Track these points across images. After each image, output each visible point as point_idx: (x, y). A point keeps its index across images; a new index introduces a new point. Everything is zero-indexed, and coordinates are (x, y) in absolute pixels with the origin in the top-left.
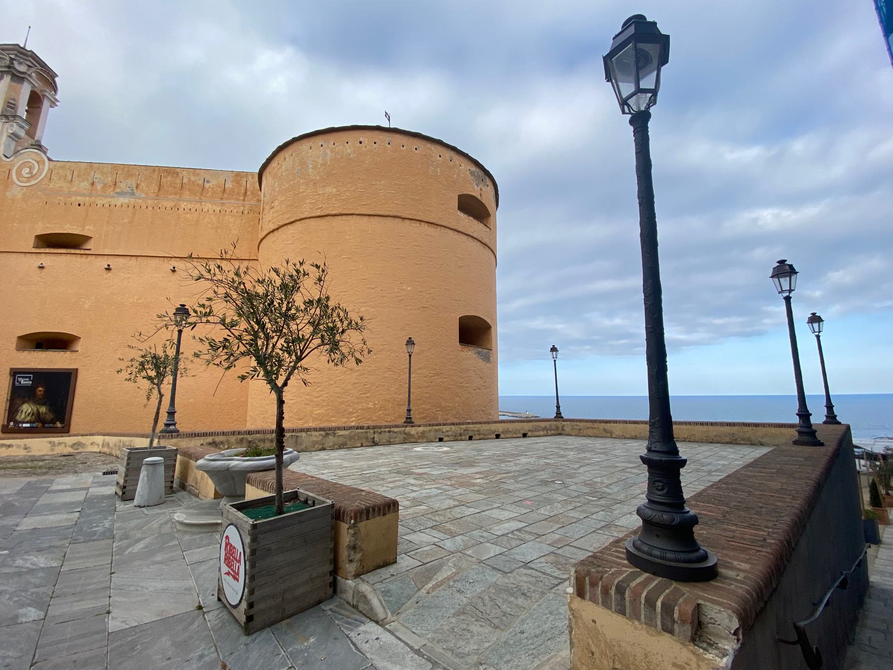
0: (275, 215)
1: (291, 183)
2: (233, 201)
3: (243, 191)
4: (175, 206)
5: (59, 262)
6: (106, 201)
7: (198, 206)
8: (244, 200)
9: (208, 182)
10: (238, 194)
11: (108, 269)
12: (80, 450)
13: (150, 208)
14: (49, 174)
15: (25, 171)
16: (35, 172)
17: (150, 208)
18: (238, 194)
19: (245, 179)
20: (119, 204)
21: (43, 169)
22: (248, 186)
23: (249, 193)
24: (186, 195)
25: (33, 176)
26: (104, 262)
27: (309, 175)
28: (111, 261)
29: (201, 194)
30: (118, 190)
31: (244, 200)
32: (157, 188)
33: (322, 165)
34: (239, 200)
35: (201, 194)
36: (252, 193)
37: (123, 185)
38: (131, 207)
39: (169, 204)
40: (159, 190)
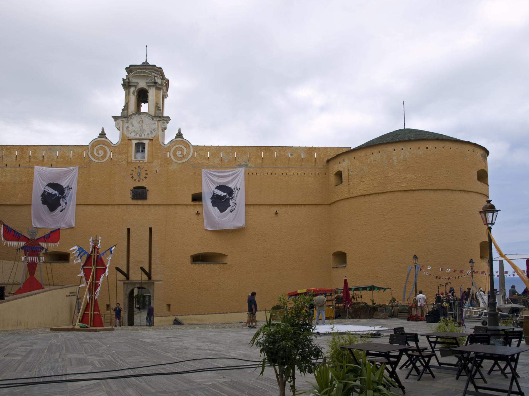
3: (314, 160)
15: (179, 153)
16: (185, 154)
23: (317, 161)
25: (184, 157)
29: (289, 164)
35: (289, 164)
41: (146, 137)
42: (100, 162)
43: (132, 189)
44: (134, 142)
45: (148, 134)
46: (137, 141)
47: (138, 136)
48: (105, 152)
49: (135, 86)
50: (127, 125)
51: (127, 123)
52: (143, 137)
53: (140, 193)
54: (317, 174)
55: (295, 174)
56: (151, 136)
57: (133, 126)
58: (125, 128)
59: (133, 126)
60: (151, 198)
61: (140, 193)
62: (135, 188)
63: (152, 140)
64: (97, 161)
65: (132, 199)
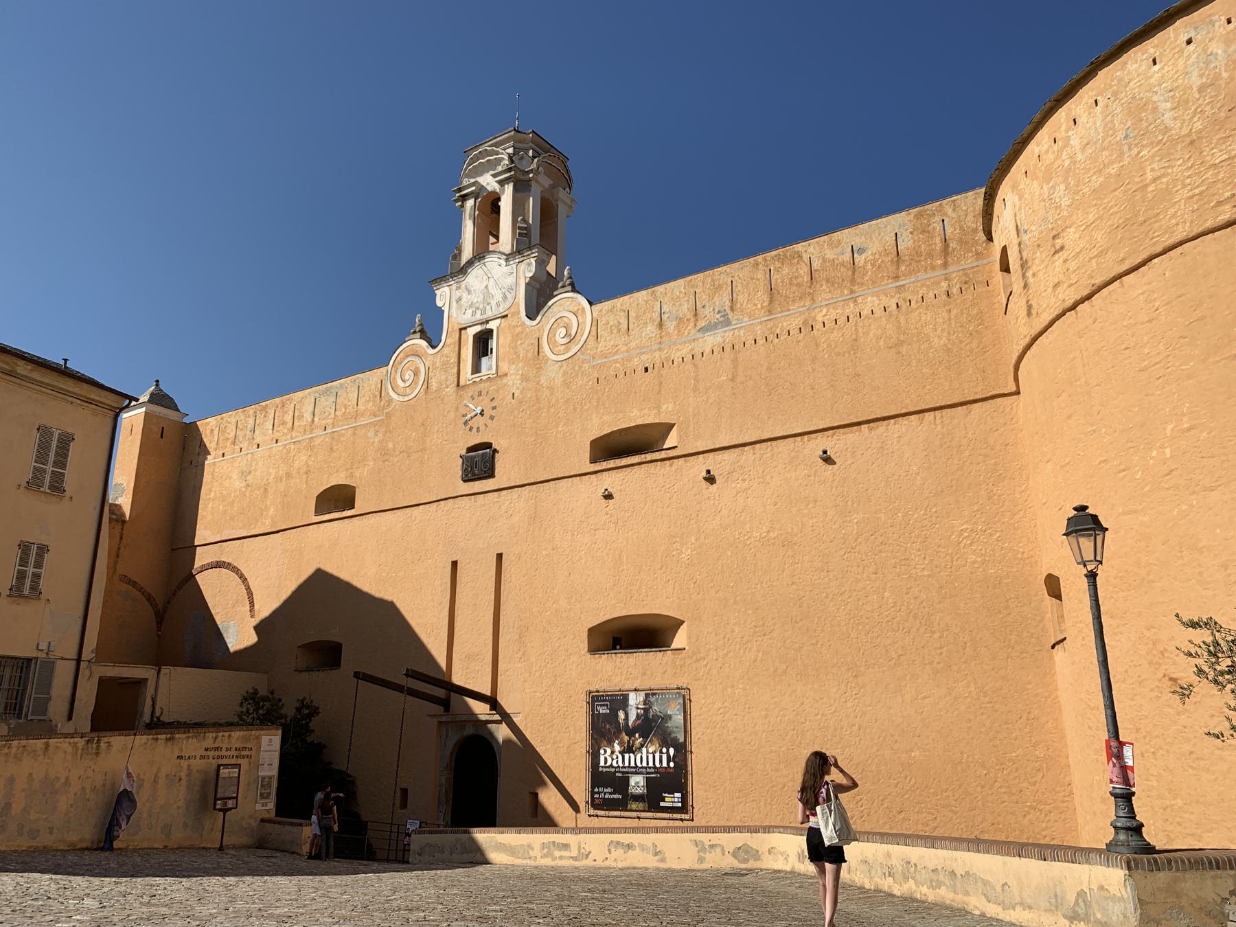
0: (1072, 265)
1: (1113, 170)
2: (921, 276)
4: (805, 322)
5: (629, 479)
6: (685, 351)
7: (851, 309)
8: (945, 265)
9: (861, 251)
10: (930, 255)
11: (710, 479)
12: (752, 864)
13: (761, 342)
14: (594, 328)
17: (761, 342)
18: (930, 255)
19: (938, 218)
20: (708, 350)
21: (584, 322)
22: (949, 230)
23: (953, 245)
24: (824, 293)
26: (698, 467)
27: (1167, 129)
28: (711, 462)
29: (853, 281)
30: (702, 324)
31: (945, 265)
32: (766, 297)
33: (1201, 90)
34: (933, 268)
35: (853, 281)
36: (961, 241)
37: (707, 311)
38: (728, 348)
39: (794, 323)
40: (771, 301)
41: (496, 312)
42: (406, 399)
43: (464, 452)
44: (472, 331)
45: (498, 304)
46: (478, 328)
47: (478, 317)
48: (416, 373)
49: (475, 195)
50: (458, 293)
51: (458, 288)
52: (489, 314)
53: (480, 463)
54: (955, 290)
55: (879, 312)
56: (502, 310)
57: (469, 292)
58: (454, 303)
59: (469, 292)
60: (505, 470)
61: (480, 463)
62: (470, 450)
63: (506, 316)
64: (401, 399)
65: (466, 480)
